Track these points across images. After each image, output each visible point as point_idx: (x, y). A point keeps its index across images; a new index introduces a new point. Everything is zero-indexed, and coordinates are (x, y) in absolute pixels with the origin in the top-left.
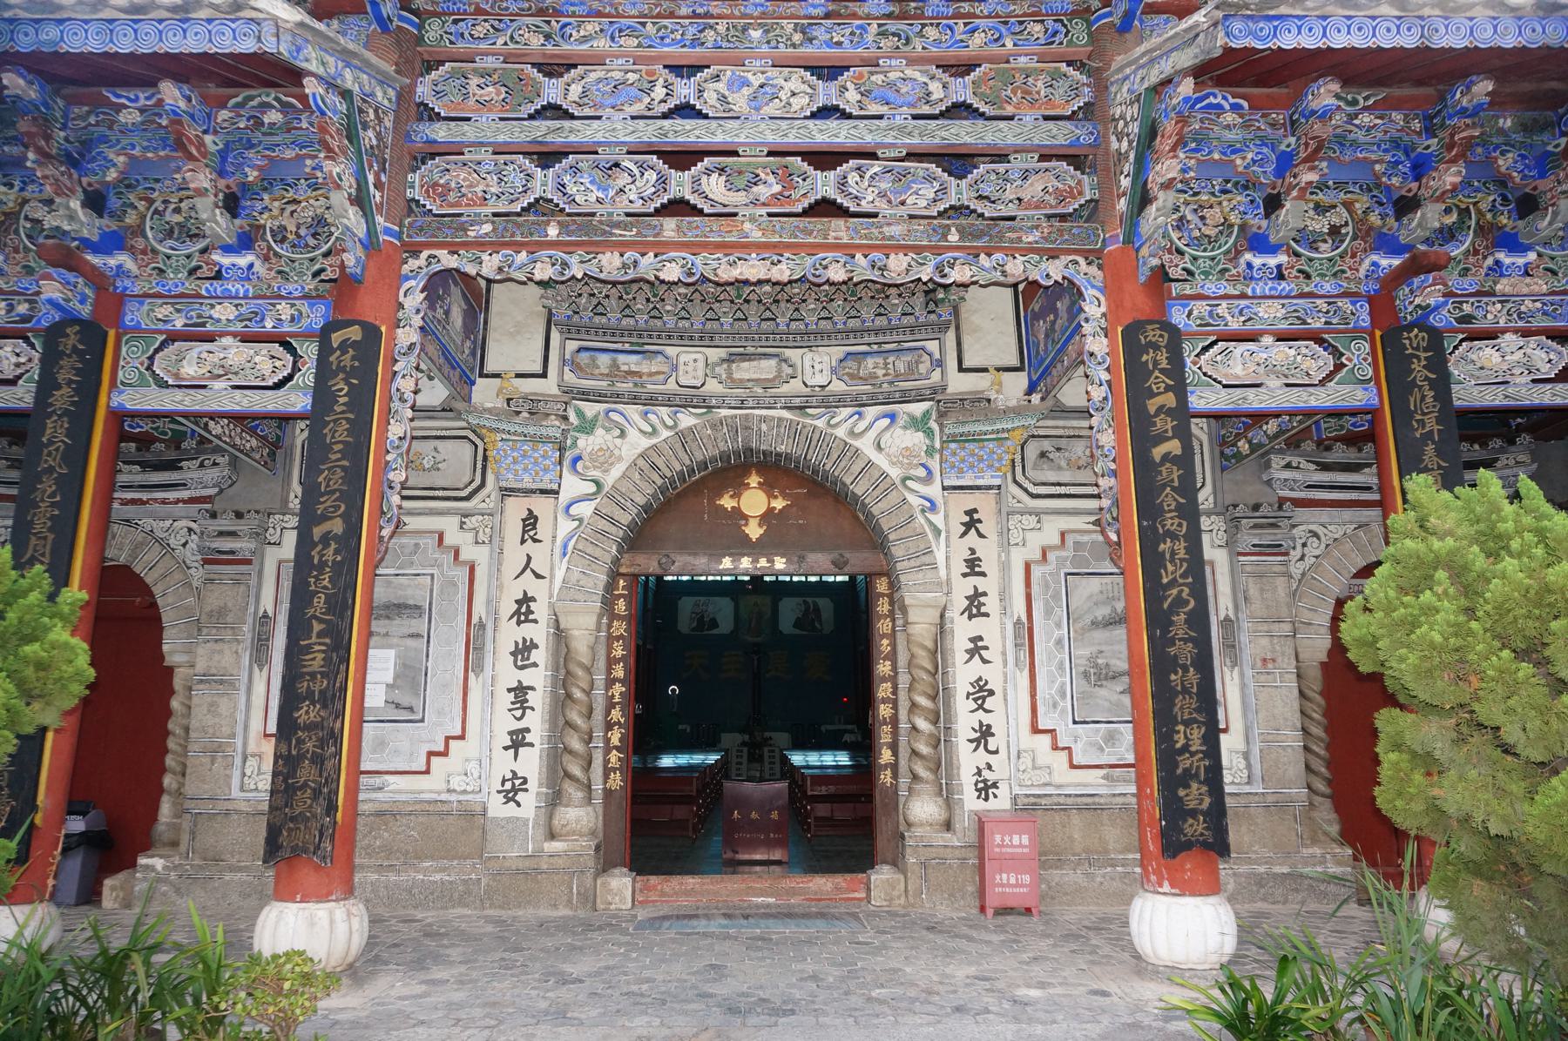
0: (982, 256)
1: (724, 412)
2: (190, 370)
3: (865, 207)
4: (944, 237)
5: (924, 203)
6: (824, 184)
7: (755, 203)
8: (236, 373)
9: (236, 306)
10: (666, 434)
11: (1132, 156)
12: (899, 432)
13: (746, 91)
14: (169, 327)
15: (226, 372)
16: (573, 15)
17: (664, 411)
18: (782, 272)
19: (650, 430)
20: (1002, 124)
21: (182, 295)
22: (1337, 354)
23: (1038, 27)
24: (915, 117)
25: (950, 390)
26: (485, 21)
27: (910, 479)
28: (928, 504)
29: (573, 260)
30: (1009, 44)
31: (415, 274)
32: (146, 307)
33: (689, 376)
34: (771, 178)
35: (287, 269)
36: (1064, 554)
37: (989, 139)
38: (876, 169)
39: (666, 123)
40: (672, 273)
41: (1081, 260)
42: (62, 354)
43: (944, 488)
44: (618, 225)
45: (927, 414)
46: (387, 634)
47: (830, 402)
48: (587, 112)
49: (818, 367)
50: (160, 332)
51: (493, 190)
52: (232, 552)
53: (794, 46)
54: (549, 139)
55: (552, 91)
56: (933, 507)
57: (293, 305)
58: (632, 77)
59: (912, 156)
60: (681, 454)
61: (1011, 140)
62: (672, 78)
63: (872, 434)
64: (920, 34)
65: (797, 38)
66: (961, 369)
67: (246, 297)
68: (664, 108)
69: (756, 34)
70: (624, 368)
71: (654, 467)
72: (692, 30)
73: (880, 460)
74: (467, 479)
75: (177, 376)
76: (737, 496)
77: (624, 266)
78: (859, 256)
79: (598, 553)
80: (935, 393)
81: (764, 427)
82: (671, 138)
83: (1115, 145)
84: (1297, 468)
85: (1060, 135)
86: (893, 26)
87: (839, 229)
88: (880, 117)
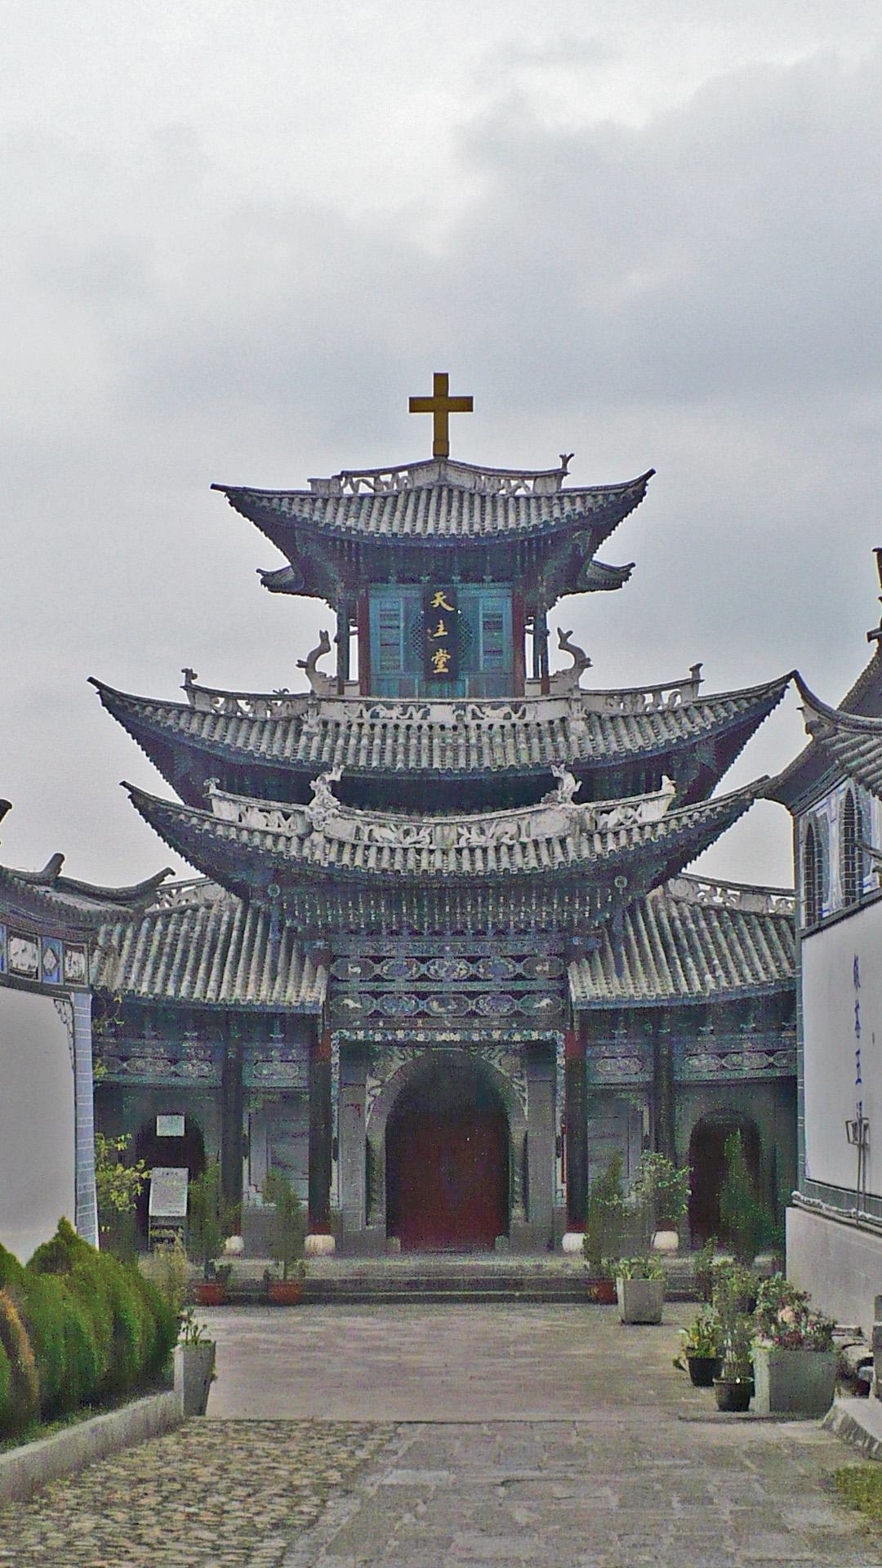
5: (505, 1010)
10: (410, 1059)
18: (457, 1037)
20: (532, 982)
37: (528, 988)
39: (418, 984)
48: (390, 978)
55: (377, 969)
56: (524, 1090)
63: (498, 1058)
64: (506, 948)
69: (448, 948)
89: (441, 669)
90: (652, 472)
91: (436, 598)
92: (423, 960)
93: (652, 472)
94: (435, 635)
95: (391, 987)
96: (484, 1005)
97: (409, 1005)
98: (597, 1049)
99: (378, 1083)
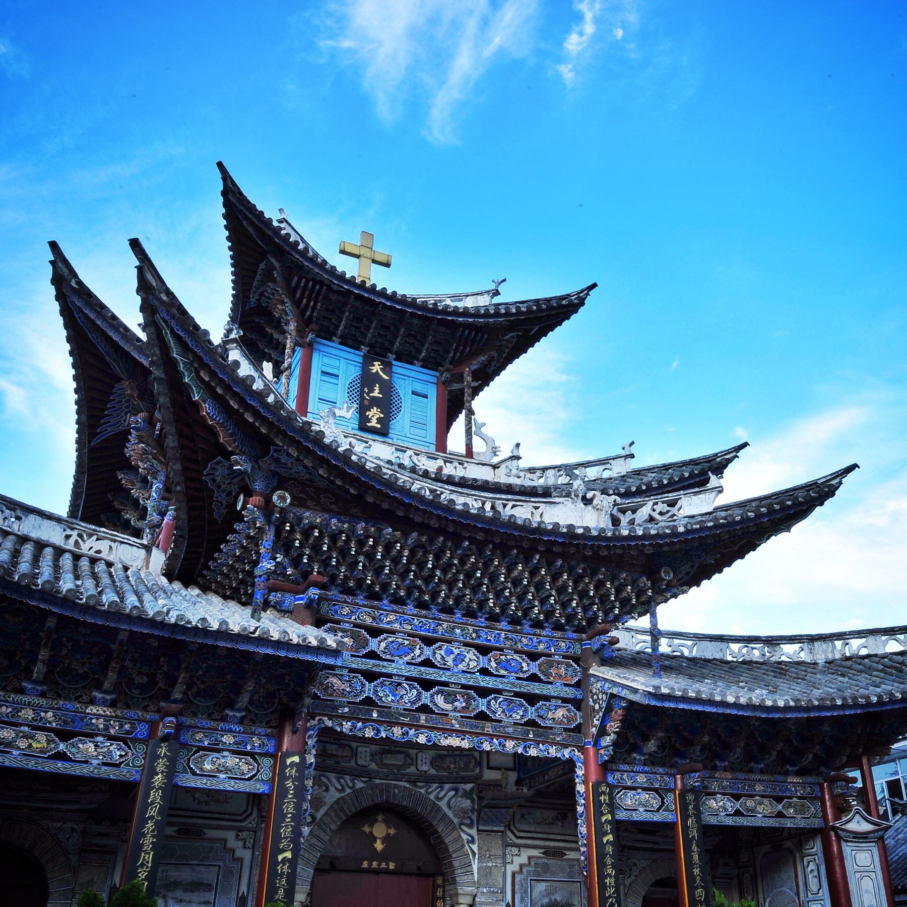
0: (541, 745)
1: (378, 781)
2: (208, 767)
3: (498, 717)
4: (528, 734)
5: (519, 717)
6: (481, 705)
7: (455, 710)
8: (230, 771)
9: (234, 736)
10: (348, 791)
11: (601, 714)
12: (459, 799)
13: (452, 656)
14: (201, 744)
15: (227, 770)
16: (385, 610)
17: (347, 777)
18: (465, 744)
19: (341, 788)
20: (550, 686)
21: (209, 729)
22: (663, 799)
23: (563, 644)
24: (518, 678)
25: (483, 778)
26: (347, 607)
27: (463, 824)
28: (470, 839)
29: (382, 729)
30: (553, 651)
31: (312, 728)
32: (190, 733)
33: (362, 760)
34: (462, 700)
35: (254, 719)
36: (530, 869)
37: (545, 692)
38: (501, 699)
39: (423, 669)
40: (422, 739)
41: (576, 750)
42: (159, 757)
43: (478, 830)
44: (401, 715)
45: (472, 790)
46: (190, 902)
47: (428, 780)
48: (388, 657)
49: (424, 761)
50: (195, 746)
51: (348, 689)
52: (105, 846)
53: (472, 639)
54: (374, 669)
55: (374, 644)
56: (473, 841)
57: (260, 739)
58: (407, 642)
59: (517, 694)
60: (356, 803)
61: (553, 694)
62: (423, 645)
63: (446, 799)
64: (520, 641)
65: (474, 635)
66: (489, 768)
67: (239, 732)
68: (419, 660)
69: (458, 631)
70: (330, 752)
71: (342, 809)
72: (433, 626)
73: (450, 814)
74: (243, 809)
75: (201, 769)
76: (371, 826)
77: (403, 734)
78: (495, 740)
79: (311, 857)
80: (476, 779)
81: (396, 791)
82: (424, 676)
83: (591, 703)
84: (630, 831)
85: (570, 693)
86: (510, 635)
87: (489, 728)
88: (503, 676)
89: (374, 423)
91: (374, 365)
92: (428, 641)
94: (371, 395)
95: (390, 669)
96: (497, 707)
97: (410, 695)
98: (618, 775)
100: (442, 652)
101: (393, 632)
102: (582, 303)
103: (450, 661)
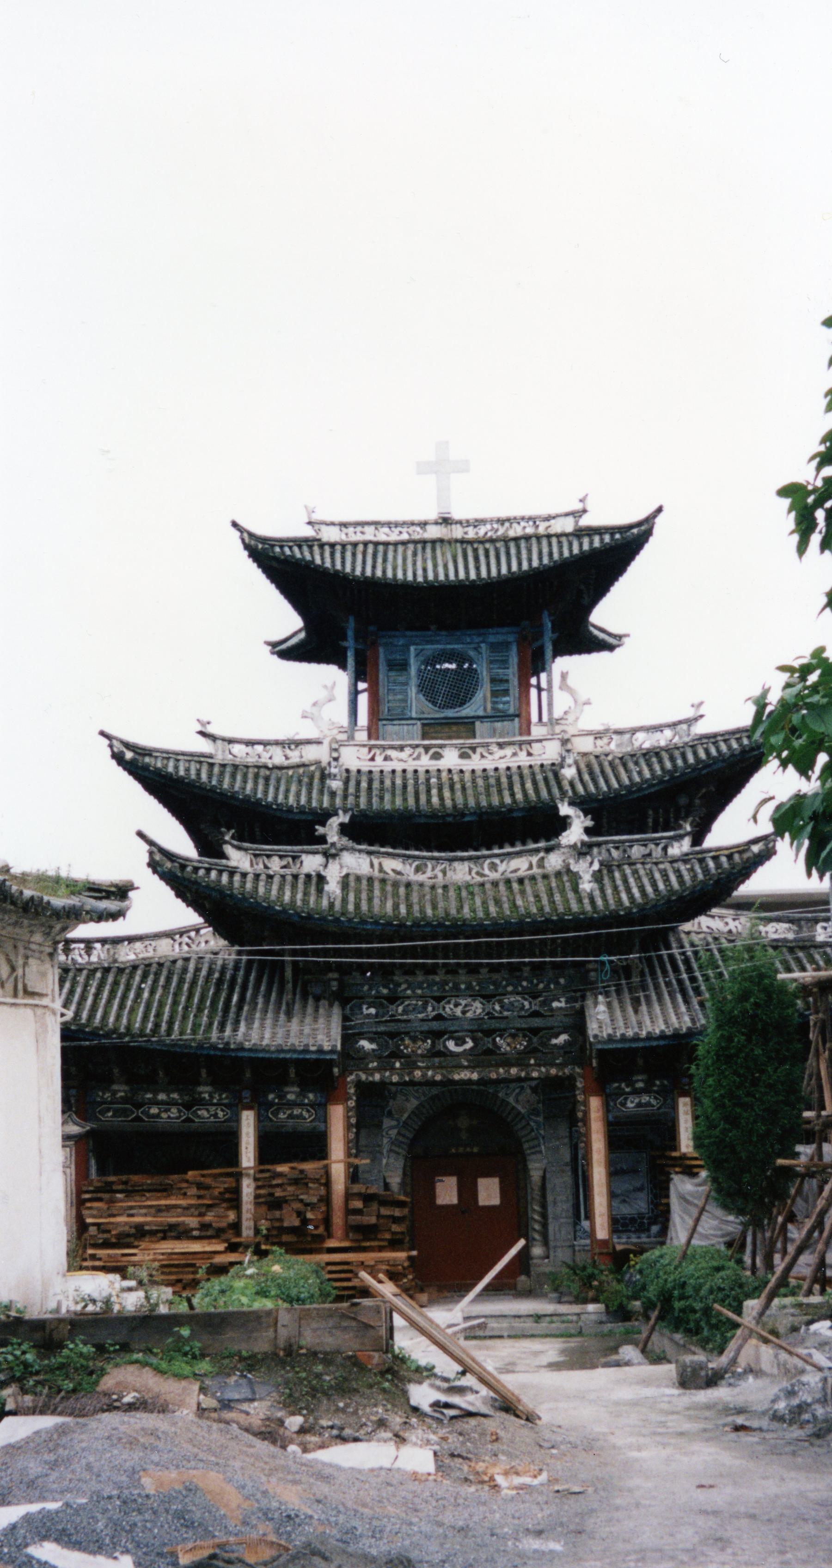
6: (487, 1043)
18: (475, 1076)
73: (519, 1107)
90: (659, 510)
93: (659, 510)
99: (394, 1123)
100: (452, 1006)
101: (408, 997)
102: (648, 534)
103: (458, 1011)
